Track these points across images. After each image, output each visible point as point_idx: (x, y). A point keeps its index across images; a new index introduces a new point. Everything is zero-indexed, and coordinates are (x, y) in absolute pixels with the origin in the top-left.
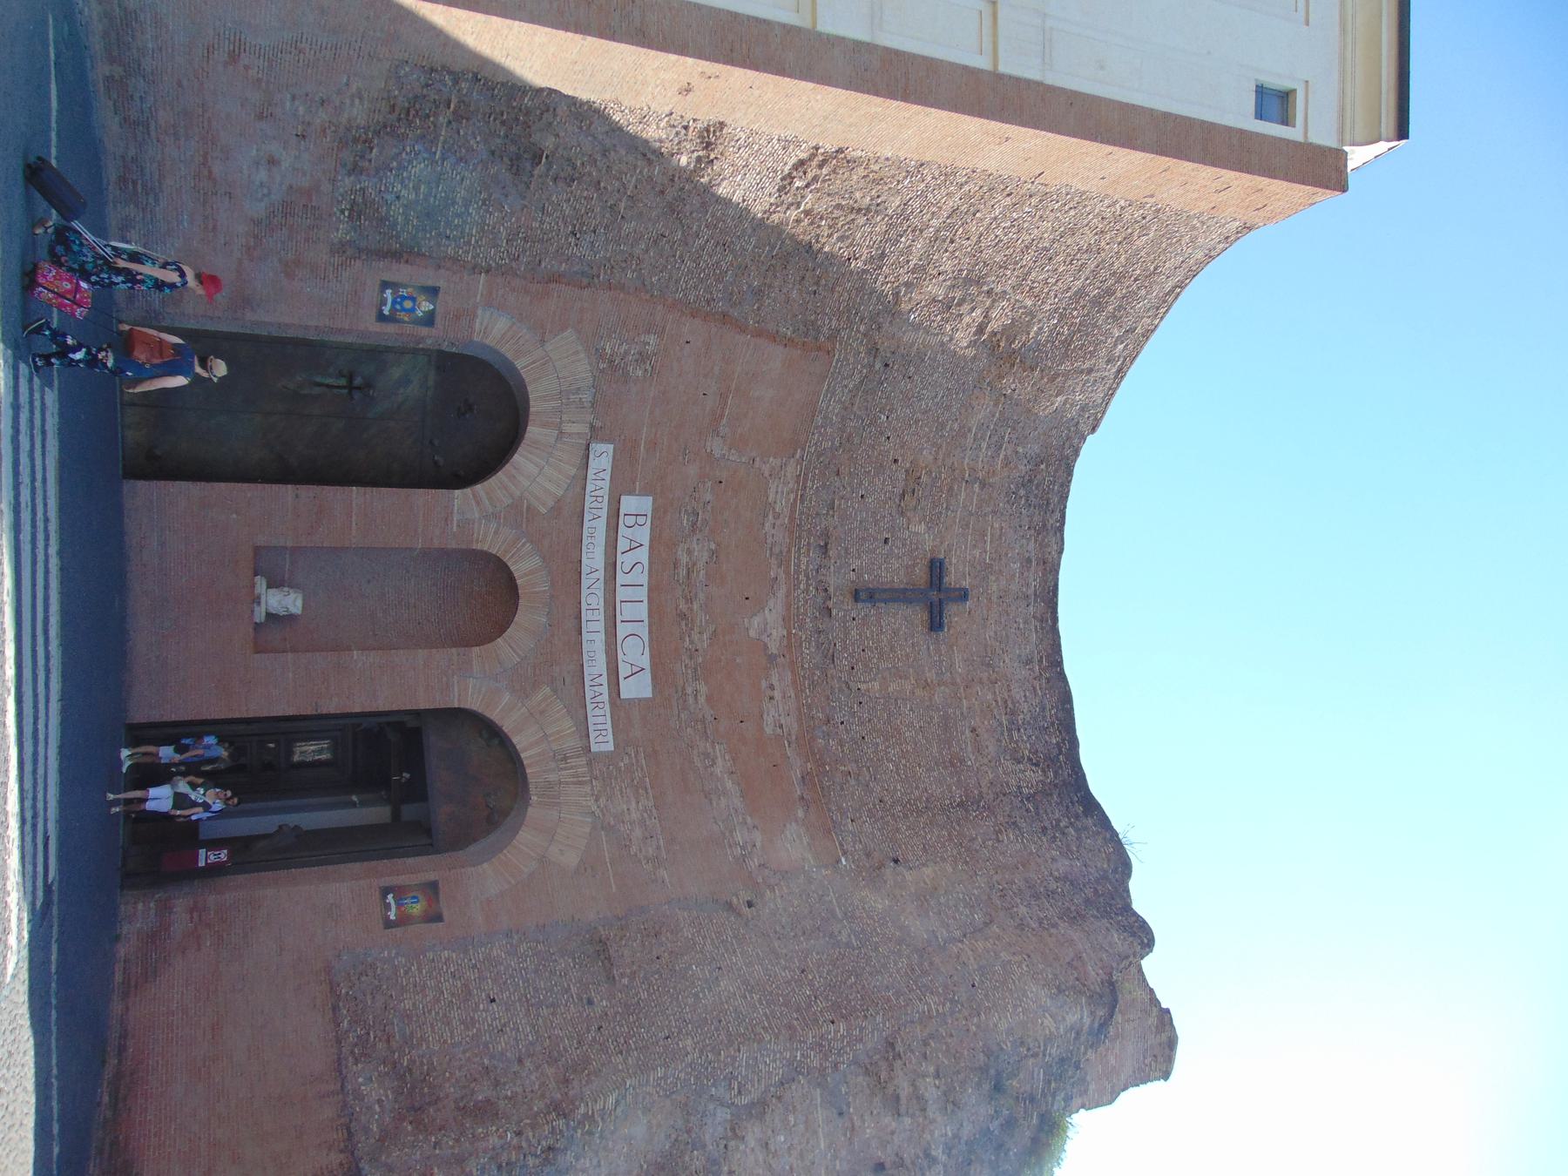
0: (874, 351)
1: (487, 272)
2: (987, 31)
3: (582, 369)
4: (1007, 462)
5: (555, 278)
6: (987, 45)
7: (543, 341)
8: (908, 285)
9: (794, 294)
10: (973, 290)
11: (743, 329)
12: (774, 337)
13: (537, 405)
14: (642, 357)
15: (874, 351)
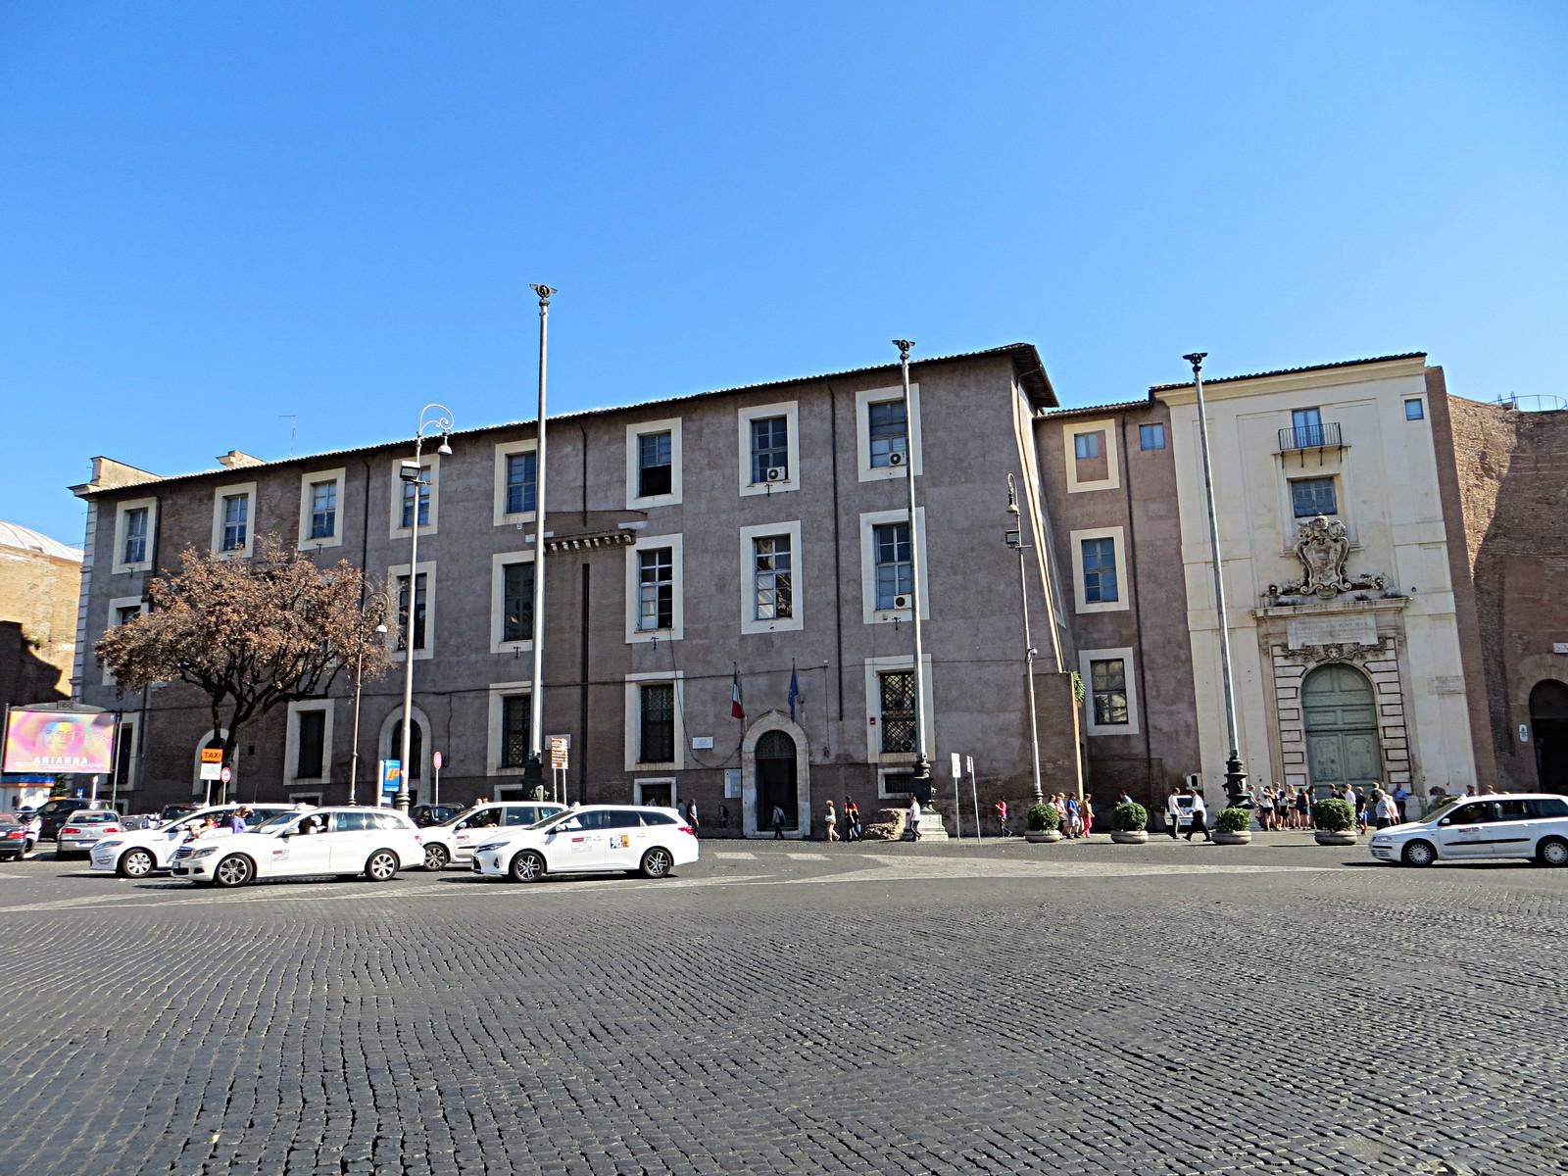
0: (1495, 536)
1: (1507, 702)
2: (1431, 546)
3: (1529, 660)
4: (1524, 451)
5: (1504, 677)
6: (1438, 545)
7: (1523, 678)
8: (1474, 529)
9: (1485, 578)
10: (1469, 499)
11: (1503, 596)
12: (1502, 583)
13: (1543, 677)
14: (1520, 637)
15: (1495, 536)
